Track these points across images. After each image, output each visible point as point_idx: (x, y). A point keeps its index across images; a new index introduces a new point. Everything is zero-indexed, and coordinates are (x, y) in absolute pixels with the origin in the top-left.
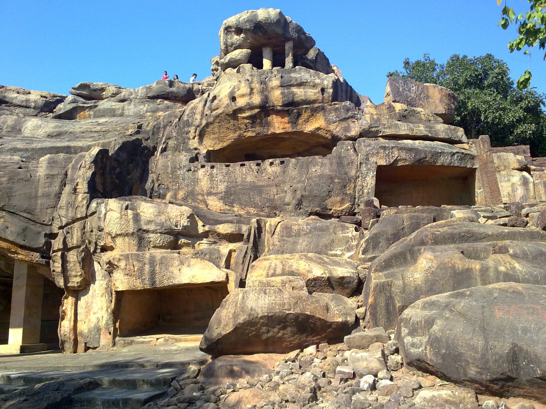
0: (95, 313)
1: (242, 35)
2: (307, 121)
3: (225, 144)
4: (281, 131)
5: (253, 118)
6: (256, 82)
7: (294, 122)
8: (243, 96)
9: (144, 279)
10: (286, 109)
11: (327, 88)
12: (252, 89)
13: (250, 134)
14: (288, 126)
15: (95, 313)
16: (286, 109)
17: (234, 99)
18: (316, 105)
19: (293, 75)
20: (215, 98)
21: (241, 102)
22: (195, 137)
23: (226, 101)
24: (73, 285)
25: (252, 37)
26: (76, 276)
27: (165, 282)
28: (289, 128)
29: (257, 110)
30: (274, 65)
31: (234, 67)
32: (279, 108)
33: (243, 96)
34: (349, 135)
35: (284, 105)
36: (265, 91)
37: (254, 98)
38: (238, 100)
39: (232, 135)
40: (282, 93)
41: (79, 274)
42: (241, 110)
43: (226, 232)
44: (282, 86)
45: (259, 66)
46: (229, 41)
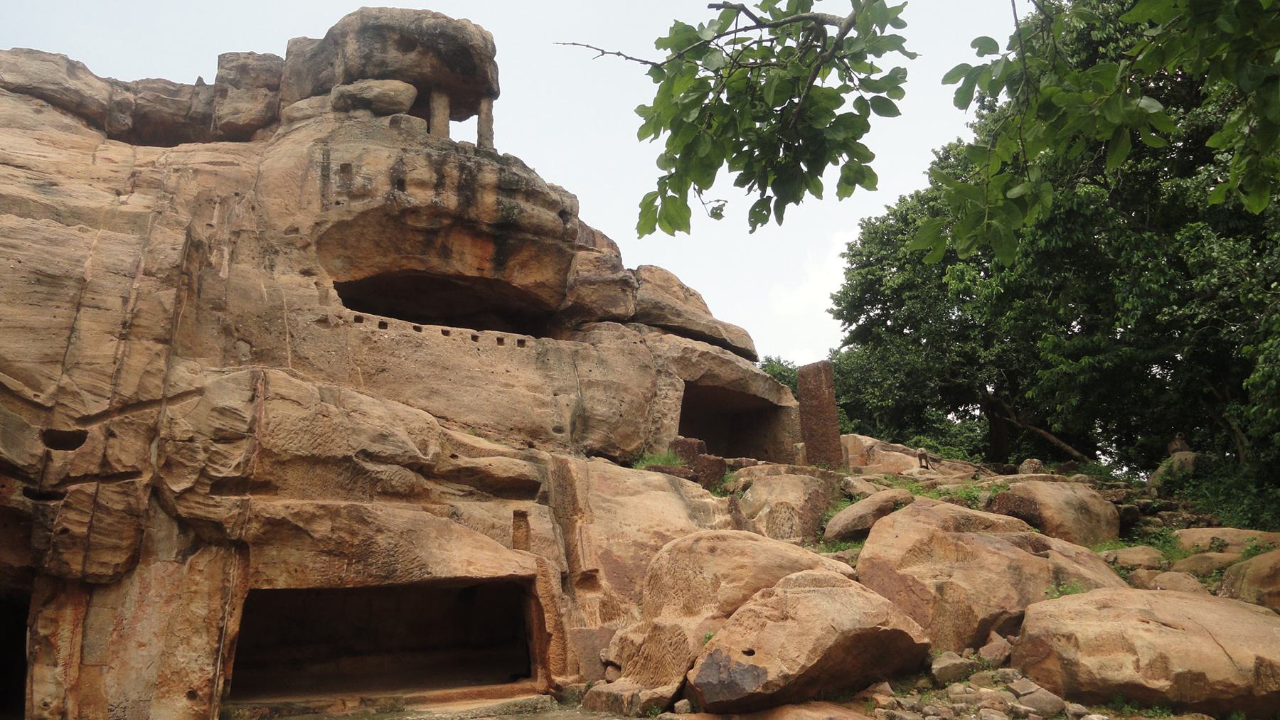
0: (141, 645)
2: (523, 265)
3: (359, 275)
4: (474, 273)
5: (431, 233)
6: (452, 165)
7: (500, 261)
8: (422, 184)
9: (371, 565)
12: (442, 177)
13: (414, 265)
14: (487, 265)
15: (141, 645)
18: (549, 241)
21: (419, 197)
22: (309, 244)
23: (383, 187)
24: (103, 570)
25: (432, 66)
26: (116, 548)
27: (417, 572)
28: (489, 273)
29: (446, 222)
32: (484, 228)
33: (422, 184)
34: (614, 311)
37: (444, 196)
38: (411, 190)
39: (378, 259)
40: (499, 203)
41: (125, 543)
42: (415, 211)
43: (505, 475)
46: (378, 56)
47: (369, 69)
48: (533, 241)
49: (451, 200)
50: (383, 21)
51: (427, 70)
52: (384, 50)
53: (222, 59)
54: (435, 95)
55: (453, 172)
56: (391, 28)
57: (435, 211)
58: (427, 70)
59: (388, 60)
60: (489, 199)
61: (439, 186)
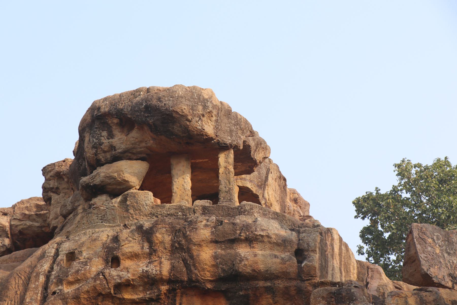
1: (135, 134)
8: (134, 256)
10: (224, 287)
11: (308, 250)
16: (224, 287)
17: (114, 261)
19: (240, 220)
20: (71, 256)
21: (131, 269)
25: (154, 139)
30: (197, 195)
31: (114, 195)
33: (134, 256)
35: (219, 280)
36: (182, 247)
44: (216, 242)
45: (164, 192)
47: (101, 157)
48: (269, 290)
49: (164, 267)
50: (105, 109)
51: (151, 143)
52: (111, 136)
53: (45, 171)
54: (173, 162)
55: (163, 236)
56: (108, 114)
57: (150, 281)
58: (151, 143)
59: (114, 144)
60: (206, 255)
61: (152, 252)
